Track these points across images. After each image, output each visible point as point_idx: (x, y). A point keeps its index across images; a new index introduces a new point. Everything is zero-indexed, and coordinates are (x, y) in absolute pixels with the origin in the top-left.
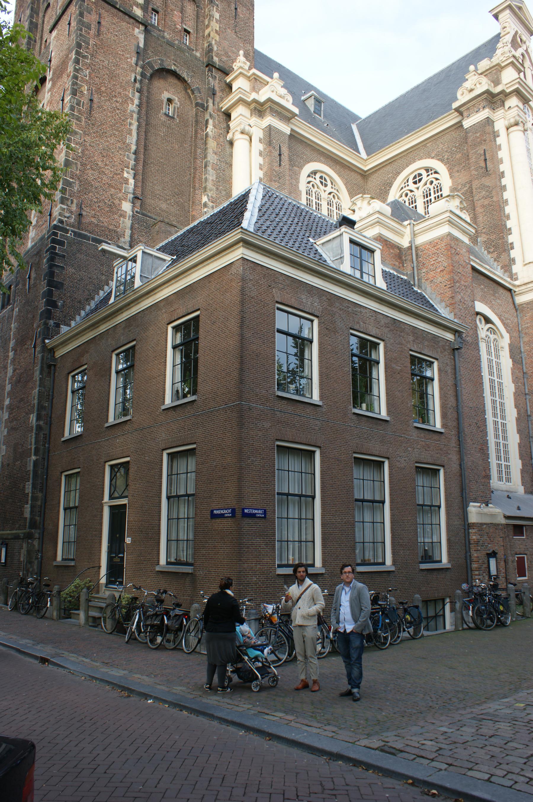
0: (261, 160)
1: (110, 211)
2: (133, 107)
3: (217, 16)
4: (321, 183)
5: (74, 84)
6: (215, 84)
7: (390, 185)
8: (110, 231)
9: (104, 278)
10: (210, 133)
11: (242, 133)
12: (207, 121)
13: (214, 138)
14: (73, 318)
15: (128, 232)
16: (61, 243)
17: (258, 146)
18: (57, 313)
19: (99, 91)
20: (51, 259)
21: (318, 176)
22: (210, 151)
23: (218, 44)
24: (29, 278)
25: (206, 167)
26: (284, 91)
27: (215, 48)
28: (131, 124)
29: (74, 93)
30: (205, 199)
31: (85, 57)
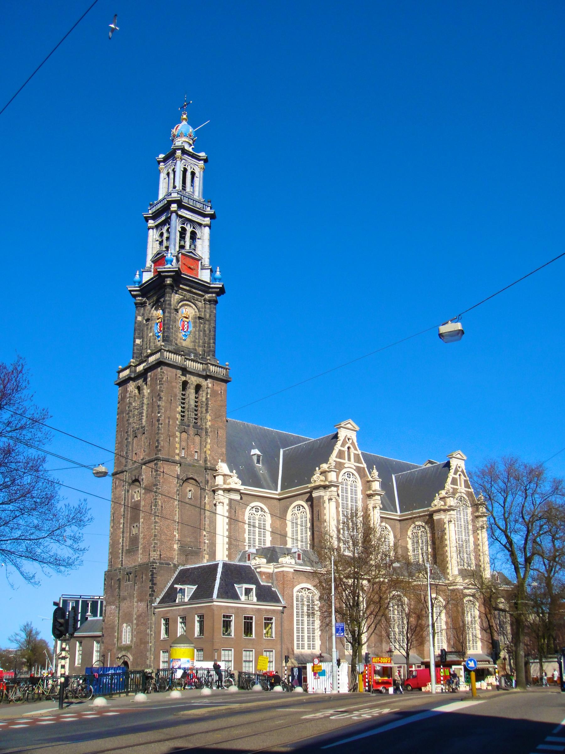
1: (170, 550)
4: (256, 511)
6: (208, 477)
7: (288, 508)
8: (170, 558)
10: (206, 502)
12: (205, 496)
14: (160, 595)
15: (177, 556)
16: (155, 568)
18: (155, 594)
20: (152, 575)
21: (254, 509)
23: (210, 455)
24: (142, 577)
25: (205, 518)
27: (208, 458)
28: (176, 511)
30: (205, 533)
31: (159, 489)
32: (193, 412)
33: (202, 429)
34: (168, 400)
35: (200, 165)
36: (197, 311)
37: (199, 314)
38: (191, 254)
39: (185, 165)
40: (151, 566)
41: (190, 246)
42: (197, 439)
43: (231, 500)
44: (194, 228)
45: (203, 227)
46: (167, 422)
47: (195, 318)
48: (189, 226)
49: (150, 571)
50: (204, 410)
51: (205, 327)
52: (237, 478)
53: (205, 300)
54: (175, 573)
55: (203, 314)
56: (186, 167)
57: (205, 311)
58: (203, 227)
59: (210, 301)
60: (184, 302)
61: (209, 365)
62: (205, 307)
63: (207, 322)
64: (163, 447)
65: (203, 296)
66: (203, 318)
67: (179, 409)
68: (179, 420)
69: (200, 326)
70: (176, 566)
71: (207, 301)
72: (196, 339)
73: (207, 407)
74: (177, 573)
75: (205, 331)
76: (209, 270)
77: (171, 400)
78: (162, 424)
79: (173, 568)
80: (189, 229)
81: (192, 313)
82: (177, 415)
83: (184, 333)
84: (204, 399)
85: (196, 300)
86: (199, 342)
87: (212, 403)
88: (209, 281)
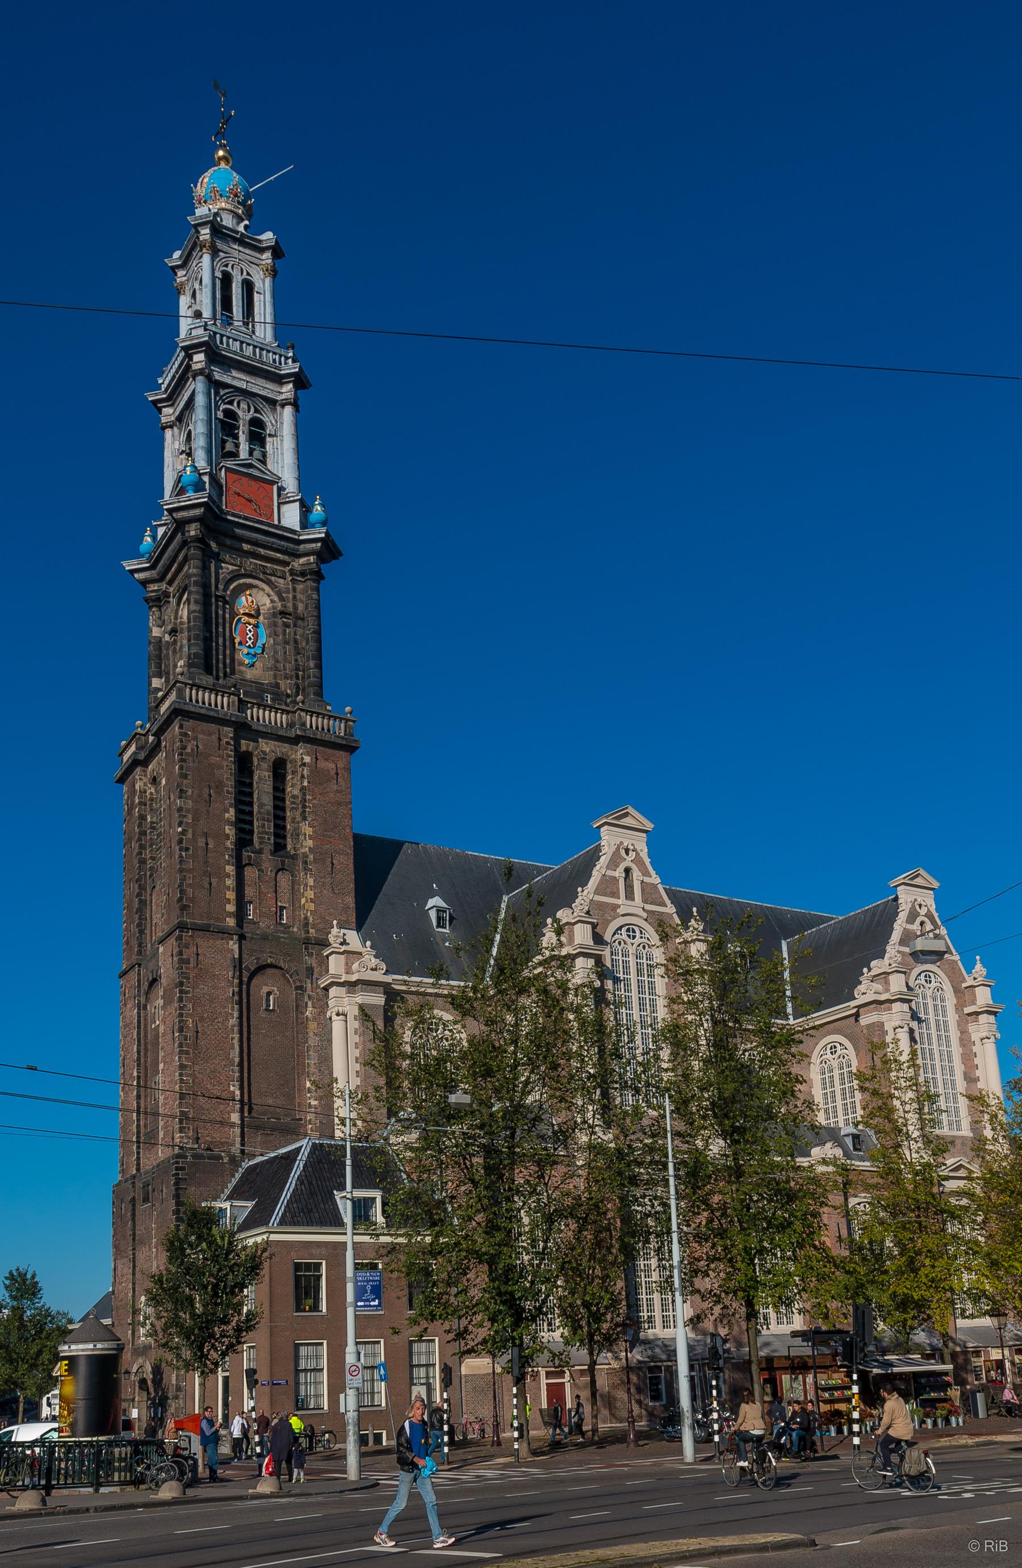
0: (357, 1039)
2: (233, 1021)
3: (311, 882)
5: (180, 1022)
6: (312, 961)
9: (220, 1187)
11: (338, 1014)
12: (307, 1003)
13: (314, 1019)
16: (182, 1169)
17: (354, 1024)
19: (202, 1019)
20: (176, 1184)
22: (311, 1034)
26: (374, 962)
27: (311, 919)
28: (233, 1039)
29: (181, 1030)
31: (187, 992)
32: (268, 821)
33: (294, 857)
34: (200, 796)
35: (264, 262)
36: (276, 599)
37: (282, 605)
38: (251, 471)
39: (226, 266)
40: (173, 1164)
41: (251, 453)
42: (284, 879)
43: (362, 1008)
44: (256, 411)
45: (278, 408)
46: (201, 842)
47: (274, 615)
48: (244, 406)
49: (173, 1175)
50: (298, 813)
51: (295, 634)
52: (376, 957)
53: (292, 572)
54: (233, 1176)
55: (290, 605)
56: (229, 269)
57: (294, 597)
58: (278, 408)
59: (303, 574)
60: (242, 581)
61: (303, 714)
62: (294, 590)
63: (300, 622)
64: (193, 900)
65: (286, 564)
66: (290, 614)
67: (231, 814)
68: (233, 838)
69: (284, 633)
70: (235, 1163)
71: (297, 575)
72: (277, 661)
73: (304, 807)
74: (238, 1176)
75: (296, 642)
76: (298, 503)
77: (210, 796)
78: (187, 849)
79: (227, 1166)
80: (244, 415)
81: (264, 605)
82: (227, 827)
83: (246, 650)
84: (296, 792)
85: (271, 575)
86: (285, 669)
87: (315, 798)
88: (298, 529)
